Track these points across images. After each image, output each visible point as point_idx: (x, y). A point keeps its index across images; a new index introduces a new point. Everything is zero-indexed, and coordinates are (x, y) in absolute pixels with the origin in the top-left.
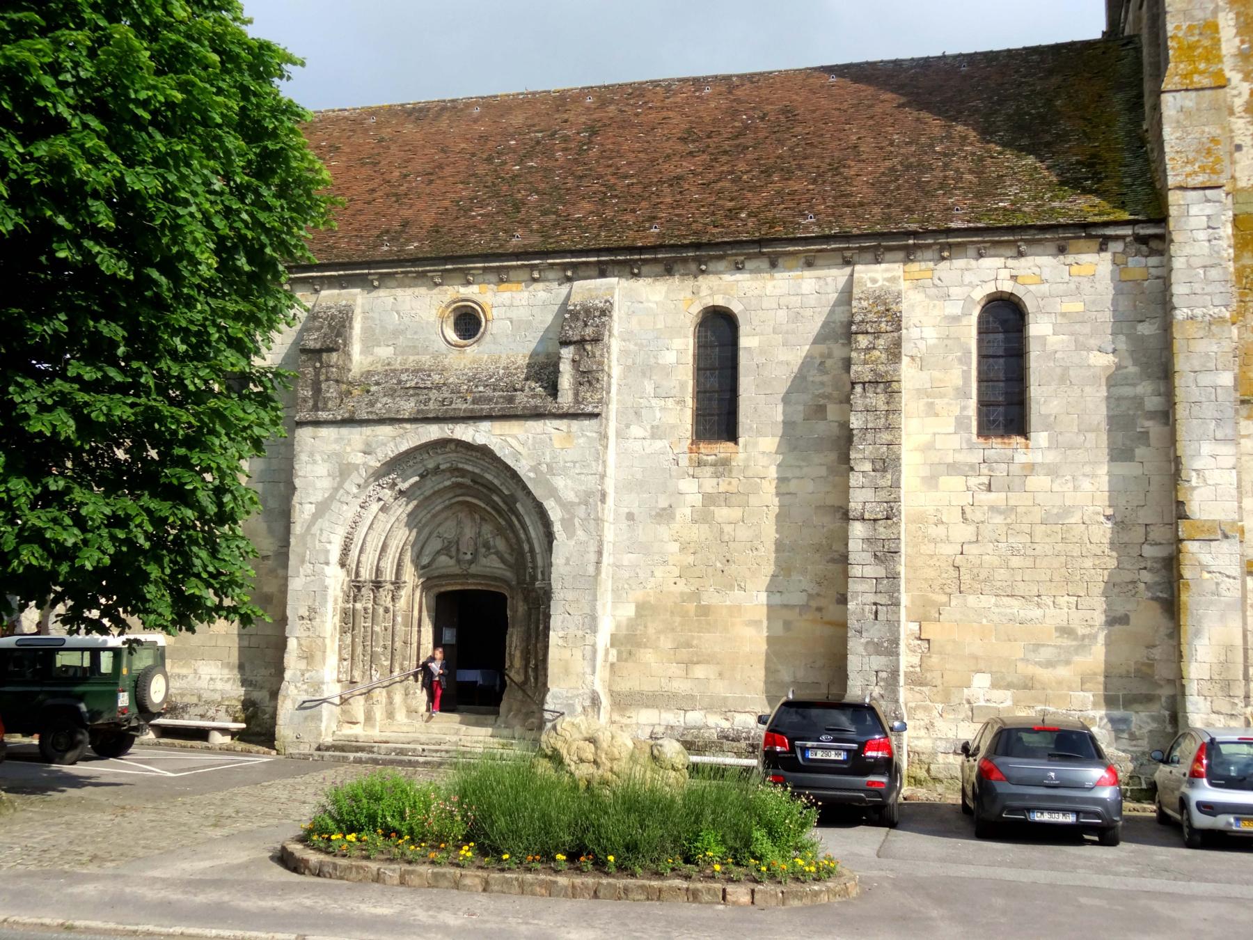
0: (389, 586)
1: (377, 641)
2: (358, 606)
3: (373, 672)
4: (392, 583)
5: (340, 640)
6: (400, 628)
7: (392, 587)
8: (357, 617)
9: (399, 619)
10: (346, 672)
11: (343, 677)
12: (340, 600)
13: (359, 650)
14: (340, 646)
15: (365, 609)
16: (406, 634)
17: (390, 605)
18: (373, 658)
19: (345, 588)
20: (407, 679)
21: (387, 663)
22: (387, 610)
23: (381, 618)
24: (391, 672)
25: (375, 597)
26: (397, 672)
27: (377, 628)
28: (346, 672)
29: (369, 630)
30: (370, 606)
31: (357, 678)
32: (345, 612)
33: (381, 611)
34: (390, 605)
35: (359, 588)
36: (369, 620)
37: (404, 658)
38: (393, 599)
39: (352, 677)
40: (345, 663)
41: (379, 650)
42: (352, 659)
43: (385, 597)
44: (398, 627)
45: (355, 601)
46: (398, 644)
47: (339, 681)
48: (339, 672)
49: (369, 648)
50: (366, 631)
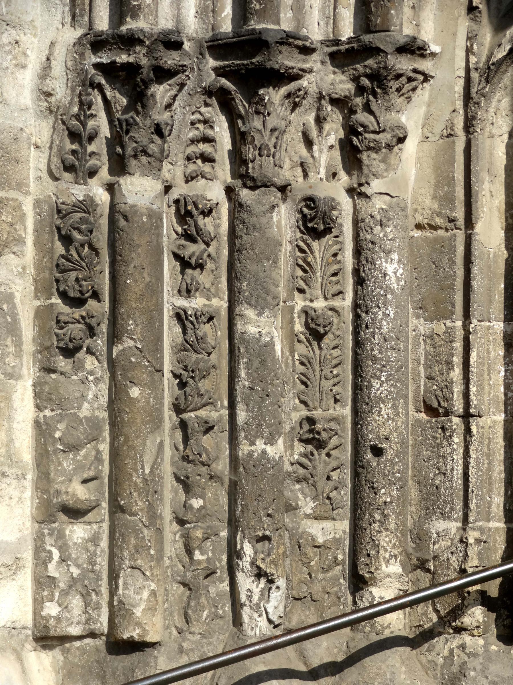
0: (322, 77)
1: (264, 392)
2: (140, 189)
3: (246, 583)
4: (342, 56)
5: (42, 397)
6: (404, 328)
7: (341, 84)
8: (136, 258)
9: (392, 269)
10: (82, 585)
11: (70, 615)
12: (35, 164)
13: (158, 449)
14: (42, 430)
15: (186, 212)
16: (438, 361)
17: (336, 191)
18: (246, 502)
19: (61, 90)
20: (450, 621)
21: (333, 530)
22: (316, 221)
23: (284, 266)
24: (358, 582)
25: (239, 138)
26: (389, 579)
27: (256, 324)
28: (82, 585)
29: (215, 334)
30: (215, 192)
31: (148, 621)
32: (66, 226)
33: (283, 220)
34: (336, 191)
35: (133, 83)
36: (214, 279)
37: (432, 503)
38: (351, 154)
39: (118, 612)
40: (78, 532)
41: (280, 451)
42: (117, 508)
43: (304, 151)
44: (385, 319)
45: (119, 166)
46: (394, 419)
47: (46, 639)
48: (43, 583)
49: (215, 444)
50: (192, 345)
